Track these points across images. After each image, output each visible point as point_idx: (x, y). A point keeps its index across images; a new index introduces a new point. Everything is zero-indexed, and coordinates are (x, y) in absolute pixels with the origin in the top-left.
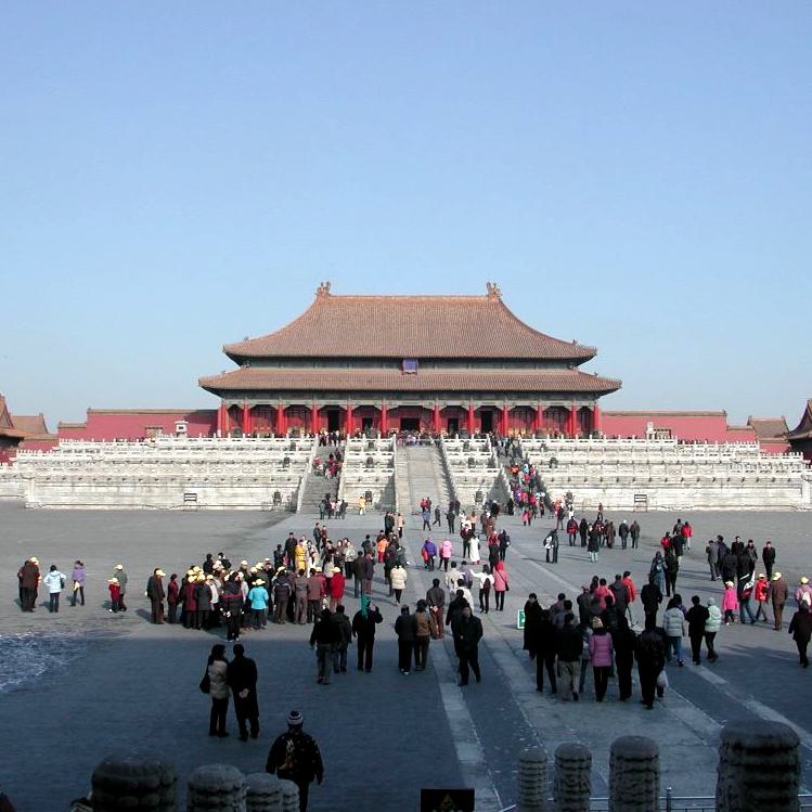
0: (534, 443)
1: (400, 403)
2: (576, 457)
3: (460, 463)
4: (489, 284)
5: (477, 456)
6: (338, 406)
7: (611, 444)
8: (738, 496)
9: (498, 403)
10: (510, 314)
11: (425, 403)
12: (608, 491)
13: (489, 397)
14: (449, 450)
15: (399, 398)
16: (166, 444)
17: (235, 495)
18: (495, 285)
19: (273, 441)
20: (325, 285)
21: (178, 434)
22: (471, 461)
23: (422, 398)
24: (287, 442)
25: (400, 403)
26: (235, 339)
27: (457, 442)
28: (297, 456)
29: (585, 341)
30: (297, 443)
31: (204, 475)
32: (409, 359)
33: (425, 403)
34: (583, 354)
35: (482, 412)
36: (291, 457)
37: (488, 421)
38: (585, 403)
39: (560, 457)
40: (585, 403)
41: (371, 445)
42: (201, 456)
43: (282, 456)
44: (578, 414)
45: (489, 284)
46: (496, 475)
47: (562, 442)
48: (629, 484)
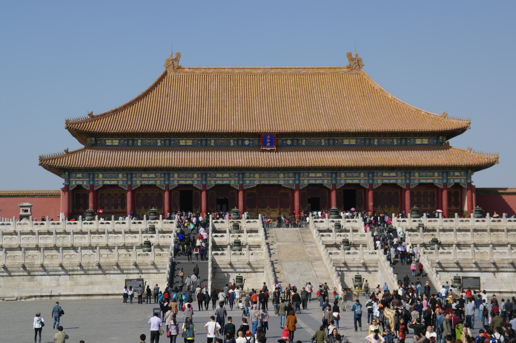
0: (410, 222)
2: (461, 238)
4: (349, 55)
5: (351, 237)
7: (494, 223)
12: (499, 275)
16: (11, 229)
17: (92, 283)
18: (357, 55)
19: (128, 223)
20: (174, 57)
21: (21, 217)
22: (346, 243)
24: (145, 224)
26: (79, 113)
27: (327, 223)
28: (155, 239)
30: (156, 226)
31: (56, 262)
36: (152, 240)
37: (351, 199)
39: (443, 238)
41: (236, 227)
42: (50, 241)
43: (140, 239)
44: (450, 192)
45: (349, 55)
47: (439, 222)
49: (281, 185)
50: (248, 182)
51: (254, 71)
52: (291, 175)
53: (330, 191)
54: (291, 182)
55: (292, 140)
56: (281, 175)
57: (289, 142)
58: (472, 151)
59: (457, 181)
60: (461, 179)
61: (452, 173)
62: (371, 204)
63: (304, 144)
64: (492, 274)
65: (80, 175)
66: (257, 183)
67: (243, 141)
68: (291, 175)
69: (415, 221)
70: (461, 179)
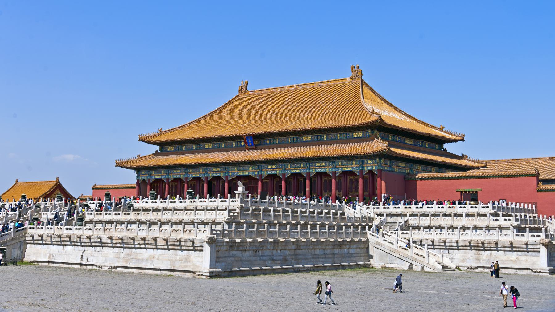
8: (152, 258)
50: (230, 174)
51: (290, 89)
52: (256, 167)
53: (305, 179)
54: (256, 173)
55: (270, 140)
56: (250, 168)
57: (268, 142)
59: (369, 168)
60: (372, 166)
61: (366, 161)
62: (260, 190)
63: (277, 142)
64: (62, 247)
65: (143, 173)
66: (236, 175)
67: (241, 142)
68: (256, 167)
70: (372, 166)
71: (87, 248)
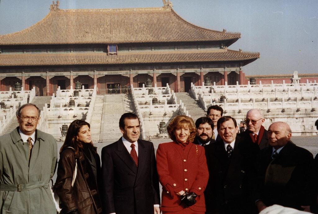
1: (105, 73)
3: (146, 103)
6: (64, 76)
9: (173, 71)
10: (179, 17)
11: (123, 73)
13: (166, 67)
14: (141, 104)
15: (105, 70)
22: (155, 101)
23: (121, 70)
25: (105, 73)
27: (144, 90)
29: (231, 29)
32: (111, 45)
33: (123, 73)
34: (231, 37)
35: (162, 78)
38: (233, 69)
40: (233, 69)
46: (175, 109)
48: (294, 114)
49: (121, 75)
58: (242, 52)
69: (207, 88)
71: (305, 119)
